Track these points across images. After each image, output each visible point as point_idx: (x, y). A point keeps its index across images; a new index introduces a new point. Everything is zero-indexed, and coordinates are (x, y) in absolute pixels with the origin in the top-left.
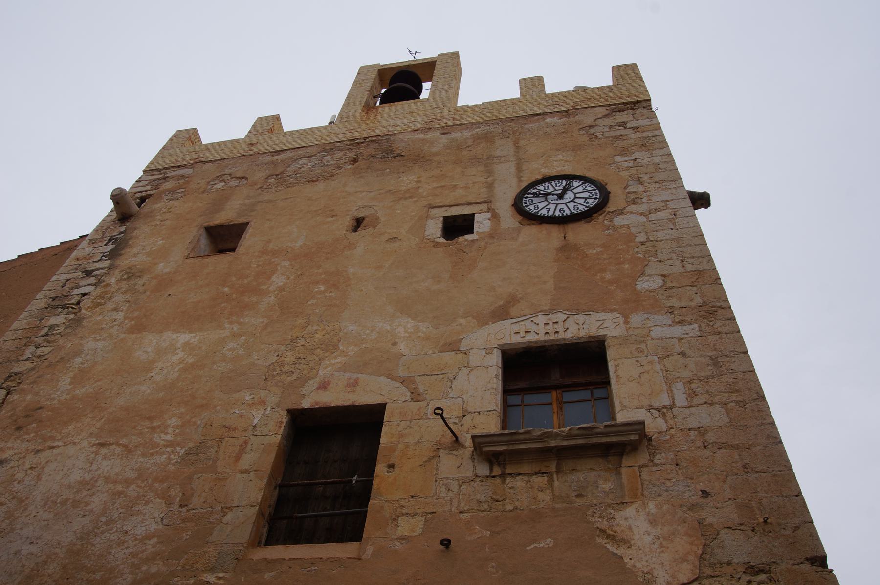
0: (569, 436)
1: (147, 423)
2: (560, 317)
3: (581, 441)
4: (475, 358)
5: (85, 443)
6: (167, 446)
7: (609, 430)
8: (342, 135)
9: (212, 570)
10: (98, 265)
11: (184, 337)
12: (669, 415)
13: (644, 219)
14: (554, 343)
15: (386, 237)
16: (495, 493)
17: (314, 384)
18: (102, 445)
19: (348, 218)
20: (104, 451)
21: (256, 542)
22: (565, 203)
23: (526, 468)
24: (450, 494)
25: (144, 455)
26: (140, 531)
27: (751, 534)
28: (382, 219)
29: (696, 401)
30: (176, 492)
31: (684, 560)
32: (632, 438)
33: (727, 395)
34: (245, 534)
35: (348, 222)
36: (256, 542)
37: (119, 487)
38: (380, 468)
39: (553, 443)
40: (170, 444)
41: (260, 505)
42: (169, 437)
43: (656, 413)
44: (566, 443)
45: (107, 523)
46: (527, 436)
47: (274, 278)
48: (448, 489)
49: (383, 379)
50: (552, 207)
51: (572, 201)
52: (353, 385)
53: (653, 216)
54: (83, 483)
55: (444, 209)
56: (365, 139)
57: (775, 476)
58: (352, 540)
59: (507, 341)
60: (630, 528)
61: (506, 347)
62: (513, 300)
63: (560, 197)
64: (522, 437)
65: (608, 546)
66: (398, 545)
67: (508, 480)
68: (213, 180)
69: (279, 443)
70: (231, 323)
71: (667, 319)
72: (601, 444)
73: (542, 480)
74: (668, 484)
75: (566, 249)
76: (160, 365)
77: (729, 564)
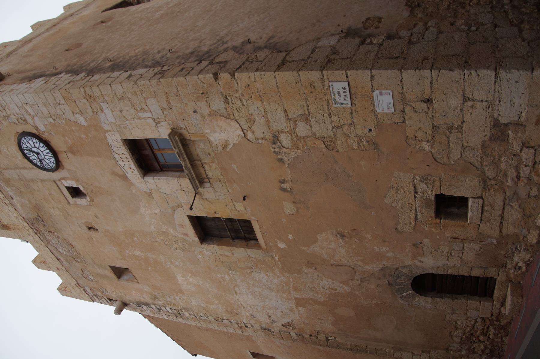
0: (184, 160)
1: (223, 283)
2: (116, 156)
3: (185, 156)
4: (153, 187)
5: (237, 297)
6: (230, 276)
7: (176, 146)
8: (35, 237)
9: (273, 258)
10: (154, 308)
11: (179, 278)
12: (158, 120)
13: (36, 118)
14: (137, 166)
15: (95, 219)
16: (217, 181)
17: (186, 238)
18: (236, 293)
19: (90, 233)
20: (238, 292)
21: (258, 246)
22: (38, 148)
23: (202, 171)
24: (222, 195)
25: (236, 281)
26: (265, 278)
27: (210, 99)
28: (85, 221)
29: (147, 109)
30: (248, 271)
31: (229, 124)
32: (177, 138)
33: (139, 97)
34: (258, 252)
35: (92, 233)
36: (258, 246)
37: (251, 285)
38: (217, 216)
39: (189, 165)
40: (229, 275)
41: (244, 248)
42: (226, 276)
43: (158, 125)
44: (187, 161)
45: (265, 286)
46: (189, 175)
47: (137, 254)
48: (220, 196)
49: (175, 216)
50: (44, 153)
51: (35, 147)
52: (182, 226)
53: (32, 114)
54: (252, 294)
55: (68, 199)
56: (32, 228)
57: (178, 85)
58: (251, 223)
59: (139, 176)
60: (220, 139)
61: (142, 175)
62: (114, 173)
63: (38, 154)
64: (190, 177)
65: (230, 147)
66: (248, 210)
67: (209, 177)
68: (89, 280)
69: (218, 245)
70: (167, 265)
71: (102, 116)
72: (184, 148)
73: (206, 167)
74: (194, 124)
75: (72, 150)
76: (195, 283)
77: (226, 109)
